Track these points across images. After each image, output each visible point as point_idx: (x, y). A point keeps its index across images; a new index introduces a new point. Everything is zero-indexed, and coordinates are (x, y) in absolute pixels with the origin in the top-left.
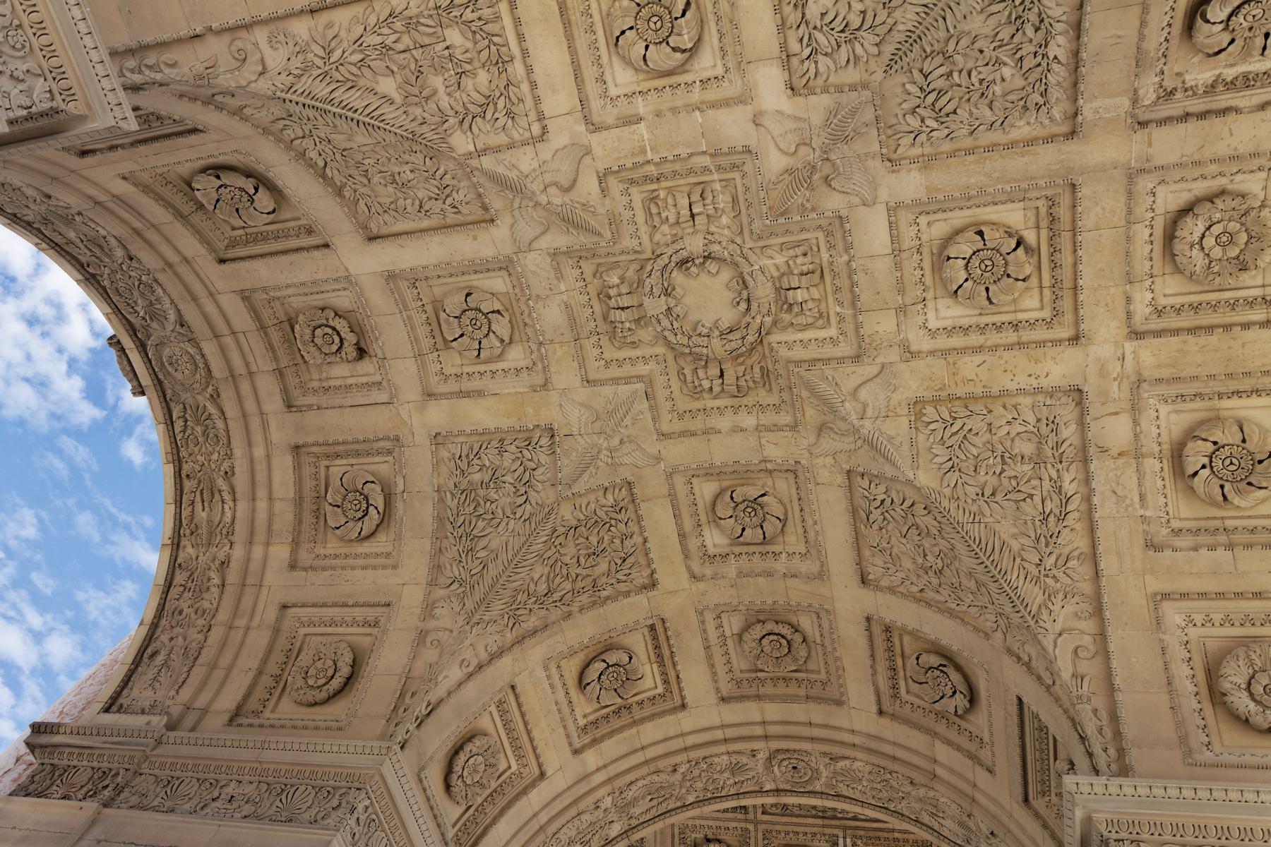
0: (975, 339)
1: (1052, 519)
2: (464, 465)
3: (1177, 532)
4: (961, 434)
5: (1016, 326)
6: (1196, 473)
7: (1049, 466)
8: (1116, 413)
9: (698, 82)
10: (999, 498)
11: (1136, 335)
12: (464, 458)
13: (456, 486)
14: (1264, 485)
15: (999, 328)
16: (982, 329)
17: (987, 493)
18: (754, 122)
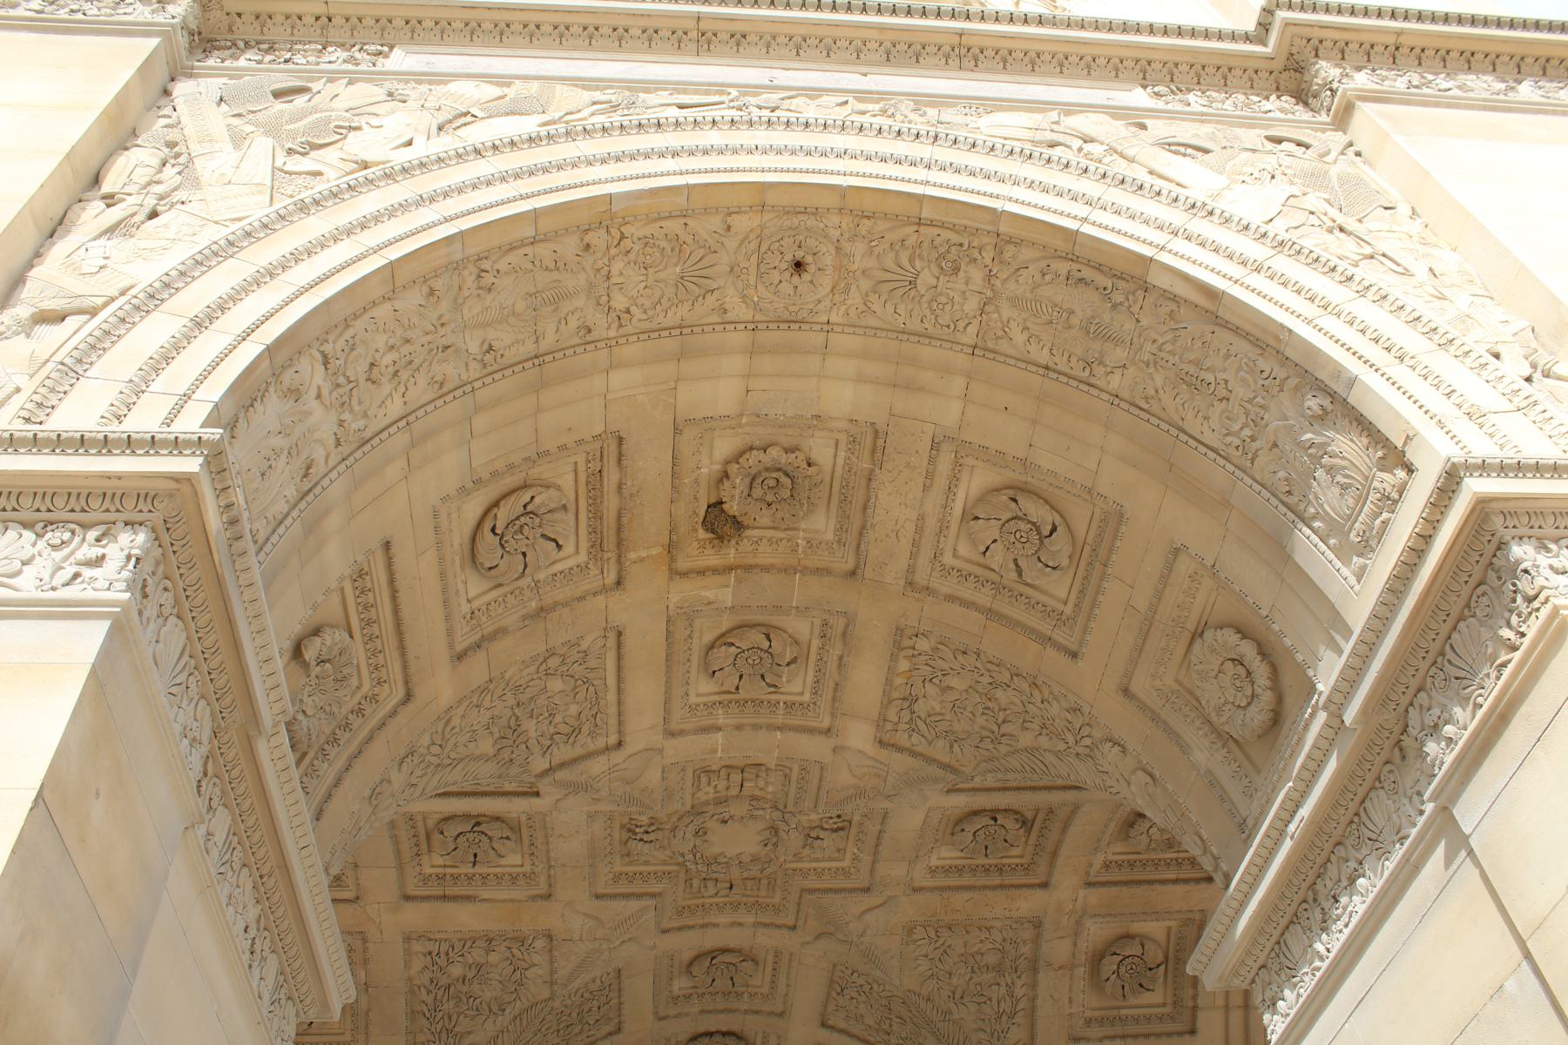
0: (967, 880)
1: (1004, 1018)
2: (442, 961)
3: (1088, 1022)
4: (941, 951)
5: (1000, 869)
6: (1108, 979)
7: (1007, 974)
8: (1062, 938)
9: (782, 704)
10: (965, 1001)
11: (1089, 884)
12: (442, 955)
13: (432, 982)
14: (1151, 988)
15: (987, 870)
16: (974, 870)
17: (958, 995)
18: (836, 747)
